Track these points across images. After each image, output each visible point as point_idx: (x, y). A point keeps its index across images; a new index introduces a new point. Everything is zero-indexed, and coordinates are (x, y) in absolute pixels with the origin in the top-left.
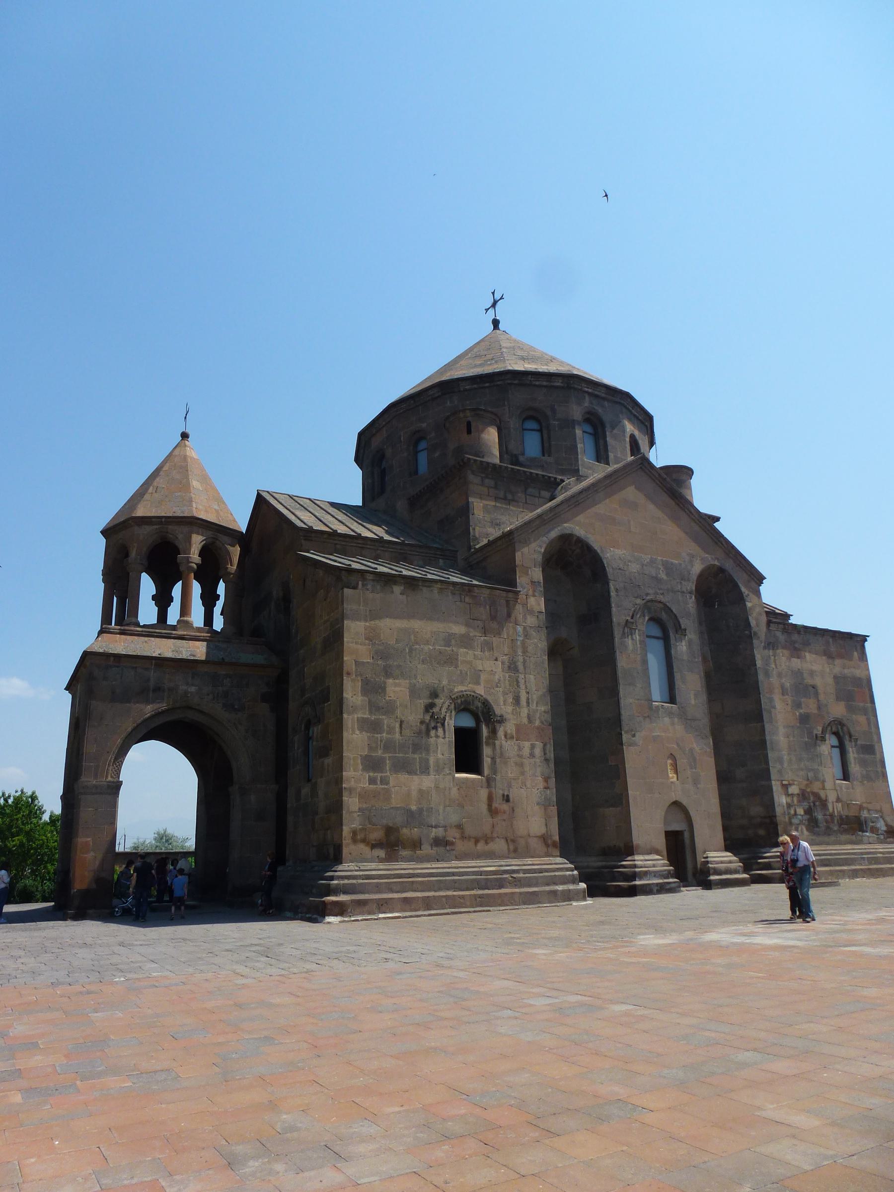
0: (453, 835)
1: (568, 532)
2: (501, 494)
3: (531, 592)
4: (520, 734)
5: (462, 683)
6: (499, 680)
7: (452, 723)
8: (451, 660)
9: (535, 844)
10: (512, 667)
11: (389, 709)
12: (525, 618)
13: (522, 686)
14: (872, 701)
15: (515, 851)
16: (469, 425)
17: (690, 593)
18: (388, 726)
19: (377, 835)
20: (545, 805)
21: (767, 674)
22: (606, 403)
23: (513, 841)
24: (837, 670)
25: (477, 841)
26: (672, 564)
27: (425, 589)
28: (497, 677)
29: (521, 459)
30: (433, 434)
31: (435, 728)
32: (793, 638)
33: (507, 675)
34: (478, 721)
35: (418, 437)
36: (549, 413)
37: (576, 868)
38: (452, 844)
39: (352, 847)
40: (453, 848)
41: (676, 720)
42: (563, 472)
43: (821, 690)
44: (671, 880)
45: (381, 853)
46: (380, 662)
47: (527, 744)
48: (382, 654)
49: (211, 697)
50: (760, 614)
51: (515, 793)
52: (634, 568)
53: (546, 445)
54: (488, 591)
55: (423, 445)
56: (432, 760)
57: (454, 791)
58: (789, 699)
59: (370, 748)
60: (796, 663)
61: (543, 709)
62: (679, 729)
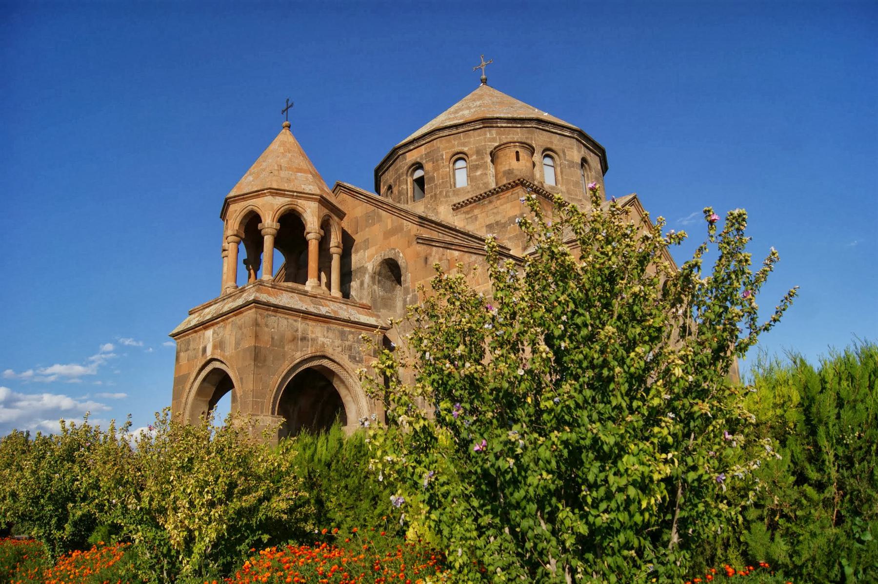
16: (517, 152)
22: (592, 154)
29: (545, 186)
30: (474, 157)
35: (460, 156)
36: (561, 155)
53: (560, 178)
55: (460, 164)
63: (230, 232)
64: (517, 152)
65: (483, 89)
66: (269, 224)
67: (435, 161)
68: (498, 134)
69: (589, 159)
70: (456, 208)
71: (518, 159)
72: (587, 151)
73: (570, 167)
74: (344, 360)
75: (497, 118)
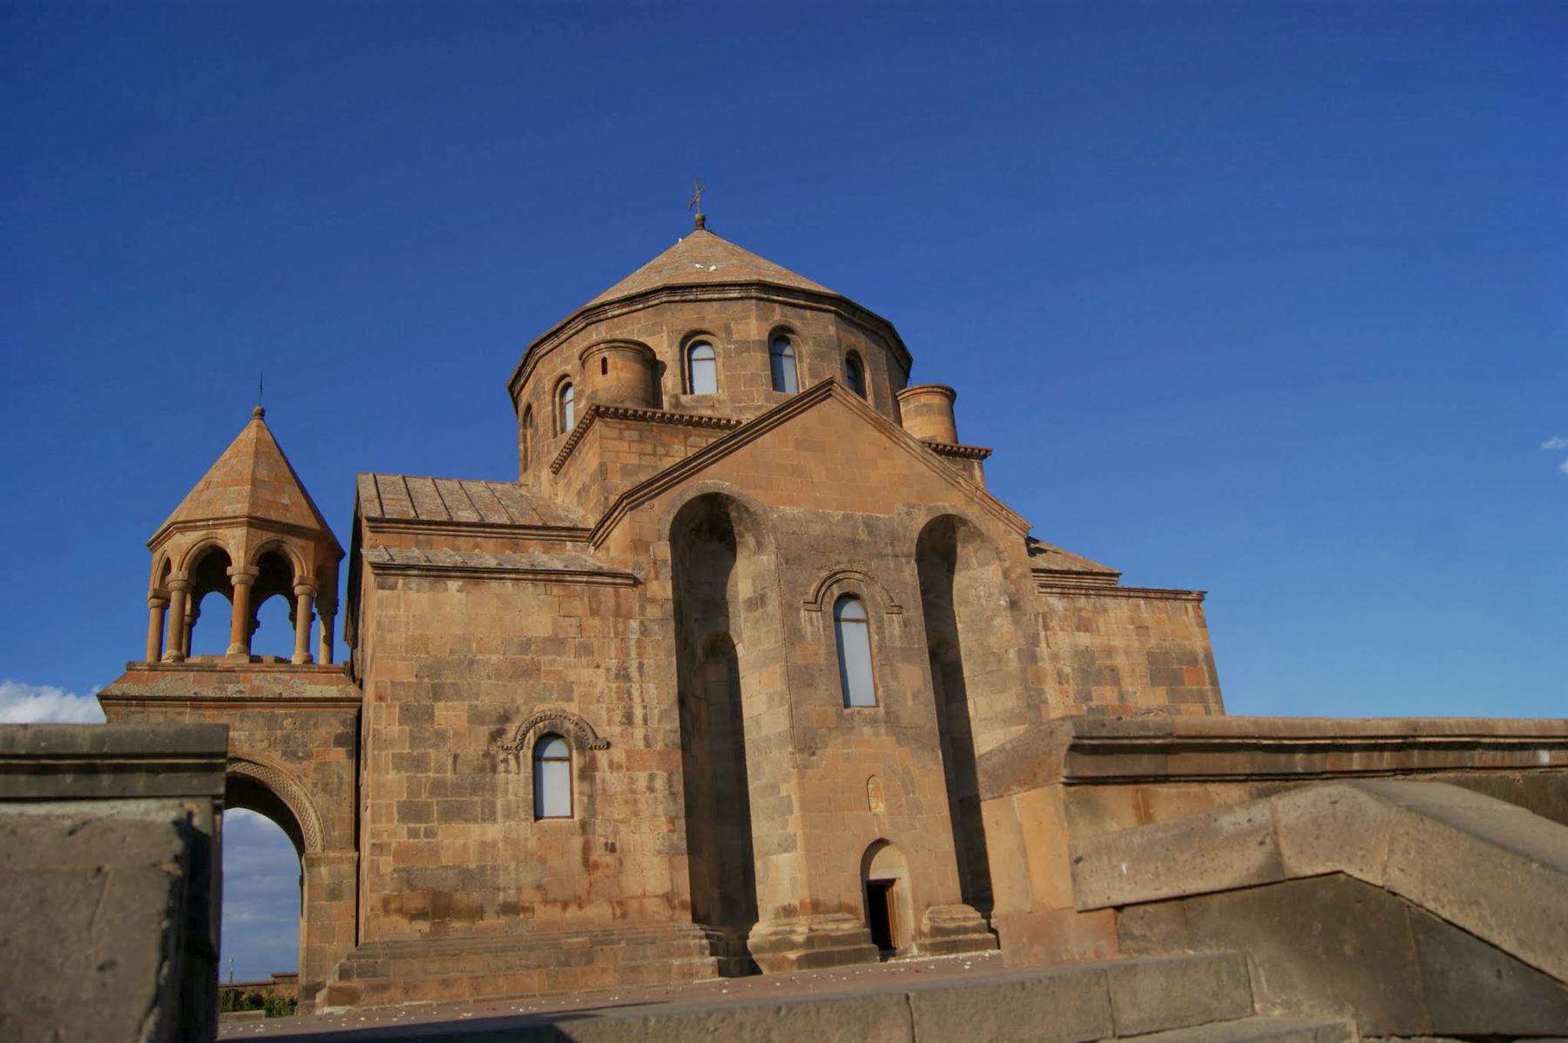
0: (530, 896)
2: (649, 449)
3: (652, 575)
4: (633, 761)
5: (543, 701)
7: (530, 753)
8: (533, 670)
9: (654, 907)
10: (623, 675)
11: (440, 736)
12: (643, 608)
13: (637, 699)
14: (1214, 681)
15: (624, 915)
16: (604, 360)
17: (908, 556)
18: (437, 761)
19: (416, 903)
20: (672, 853)
21: (1033, 657)
22: (808, 313)
23: (620, 903)
24: (1152, 642)
25: (565, 905)
26: (878, 519)
27: (493, 583)
28: (598, 690)
29: (684, 399)
31: (505, 761)
33: (614, 686)
34: (571, 751)
35: (563, 385)
37: (708, 936)
38: (525, 910)
39: (382, 919)
40: (529, 914)
41: (882, 729)
42: (741, 410)
43: (1124, 673)
44: (864, 946)
45: (424, 926)
46: (427, 680)
47: (642, 779)
49: (265, 743)
50: (1025, 576)
51: (627, 838)
52: (818, 528)
54: (585, 579)
55: (570, 394)
56: (500, 803)
57: (533, 843)
58: (1071, 688)
59: (411, 793)
60: (1084, 639)
61: (668, 727)
62: (886, 740)
63: (150, 594)
64: (604, 360)
65: (701, 236)
66: (177, 575)
67: (537, 398)
68: (610, 329)
69: (797, 324)
70: (557, 469)
71: (604, 372)
72: (789, 311)
73: (739, 352)
74: (276, 759)
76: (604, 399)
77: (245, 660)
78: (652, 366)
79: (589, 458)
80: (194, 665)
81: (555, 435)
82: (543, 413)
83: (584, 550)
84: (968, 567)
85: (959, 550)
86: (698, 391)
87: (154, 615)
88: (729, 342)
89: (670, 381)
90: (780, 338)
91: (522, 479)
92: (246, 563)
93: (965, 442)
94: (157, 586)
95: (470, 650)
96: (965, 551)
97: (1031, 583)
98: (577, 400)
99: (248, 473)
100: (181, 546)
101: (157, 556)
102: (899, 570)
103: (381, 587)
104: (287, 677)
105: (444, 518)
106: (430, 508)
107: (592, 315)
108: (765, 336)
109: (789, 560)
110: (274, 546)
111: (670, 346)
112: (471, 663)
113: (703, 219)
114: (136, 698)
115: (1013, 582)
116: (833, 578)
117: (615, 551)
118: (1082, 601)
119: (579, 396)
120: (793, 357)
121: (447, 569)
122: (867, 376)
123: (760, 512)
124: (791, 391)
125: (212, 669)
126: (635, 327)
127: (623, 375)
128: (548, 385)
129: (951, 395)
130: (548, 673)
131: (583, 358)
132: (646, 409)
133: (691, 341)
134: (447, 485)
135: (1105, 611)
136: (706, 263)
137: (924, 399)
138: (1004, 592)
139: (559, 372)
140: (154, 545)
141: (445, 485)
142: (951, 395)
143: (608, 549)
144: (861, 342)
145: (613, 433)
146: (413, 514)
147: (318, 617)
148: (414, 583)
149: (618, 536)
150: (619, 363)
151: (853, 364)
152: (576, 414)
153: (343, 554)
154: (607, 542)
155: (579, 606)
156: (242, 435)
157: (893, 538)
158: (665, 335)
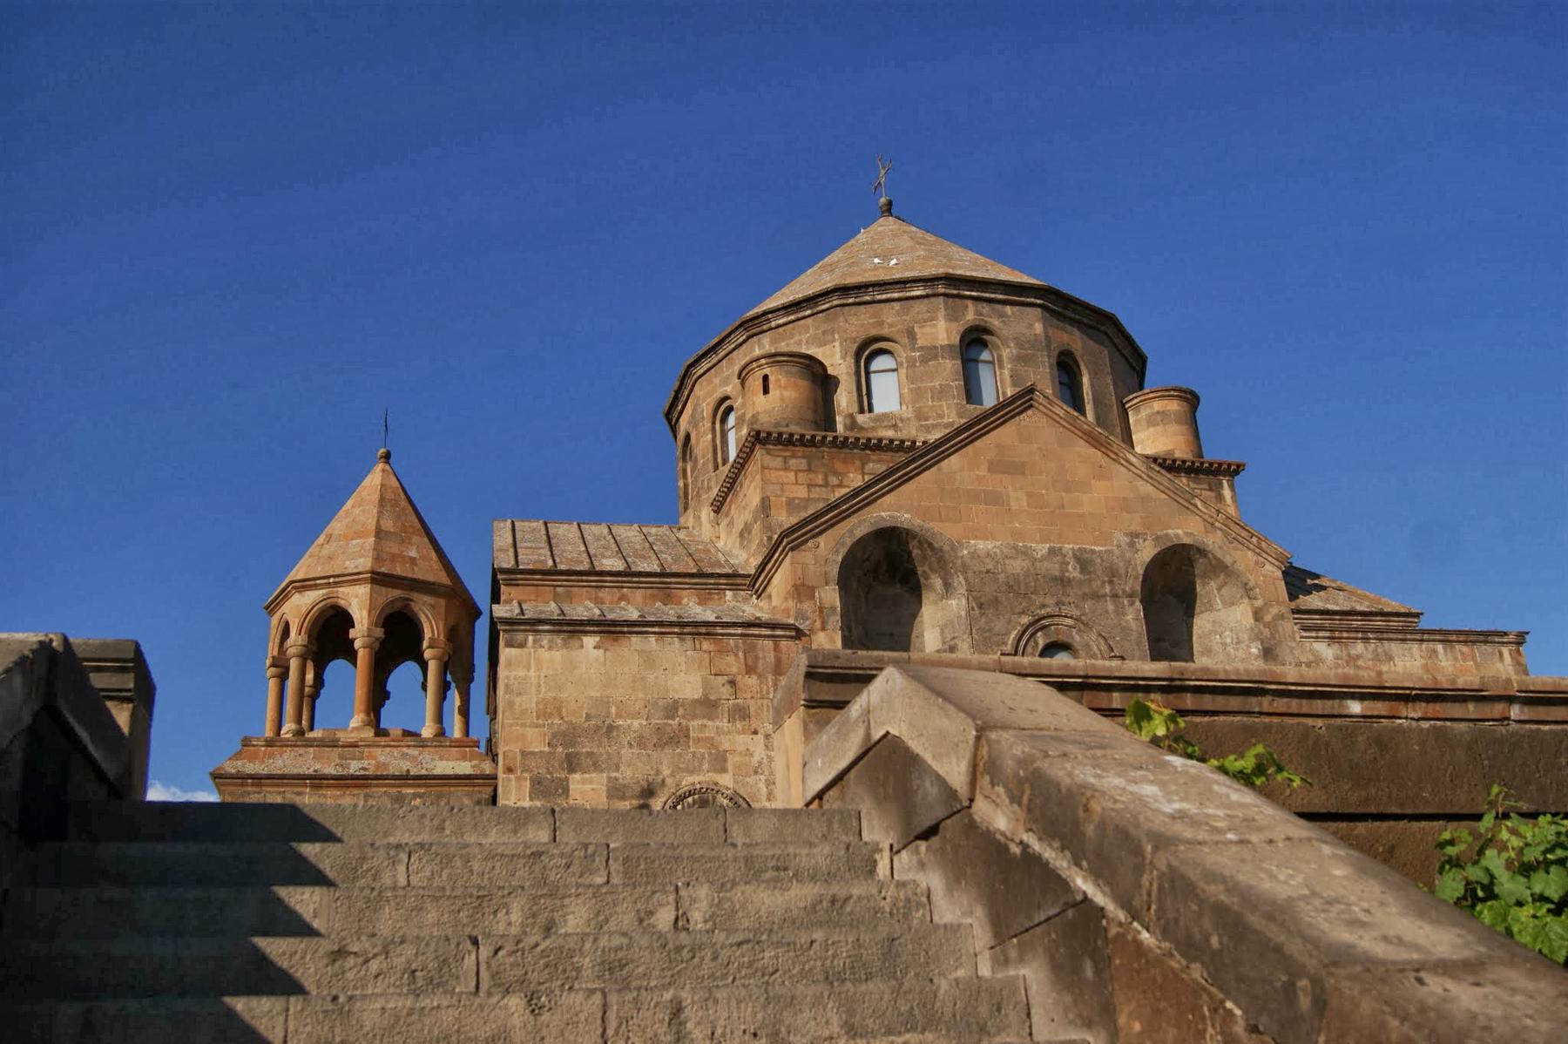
1: (889, 524)
2: (819, 479)
3: (818, 624)
5: (692, 773)
6: (760, 763)
8: (679, 738)
16: (766, 378)
17: (1131, 595)
22: (1008, 309)
26: (1093, 552)
27: (635, 639)
28: (756, 758)
29: (861, 419)
32: (1353, 652)
35: (723, 409)
42: (928, 429)
46: (560, 749)
48: (568, 737)
52: (1017, 566)
54: (739, 631)
63: (268, 662)
64: (766, 378)
65: (887, 225)
66: (296, 640)
67: (696, 426)
68: (774, 342)
69: (995, 323)
70: (718, 506)
71: (766, 391)
72: (986, 308)
73: (924, 361)
75: (765, 313)
76: (765, 423)
77: (369, 733)
78: (823, 382)
79: (751, 493)
80: (314, 739)
81: (716, 468)
82: (702, 444)
83: (746, 600)
84: (1210, 607)
85: (1198, 588)
86: (879, 408)
87: (273, 684)
88: (913, 349)
89: (844, 399)
90: (974, 341)
91: (682, 520)
92: (370, 624)
93: (1212, 455)
94: (275, 653)
95: (608, 715)
96: (1207, 589)
97: (1289, 626)
98: (738, 426)
99: (371, 523)
100: (300, 606)
101: (275, 620)
102: (1120, 612)
103: (509, 645)
104: (414, 752)
105: (585, 566)
106: (571, 554)
107: (753, 326)
108: (956, 340)
109: (982, 604)
110: (398, 605)
111: (844, 358)
112: (610, 729)
113: (890, 203)
114: (252, 777)
115: (1267, 625)
116: (1037, 625)
117: (776, 601)
118: (1359, 647)
119: (740, 420)
120: (992, 363)
121: (581, 623)
122: (1085, 380)
123: (946, 548)
124: (989, 401)
125: (333, 744)
126: (803, 338)
127: (787, 394)
128: (707, 408)
129: (1192, 400)
130: (699, 740)
131: (742, 376)
132: (817, 431)
133: (868, 351)
134: (594, 531)
135: (1391, 658)
136: (886, 257)
137: (1157, 405)
138: (1257, 637)
139: (718, 395)
140: (271, 608)
141: (591, 530)
142: (1192, 400)
143: (770, 596)
144: (1075, 340)
145: (778, 462)
146: (550, 563)
147: (453, 685)
148: (545, 640)
149: (780, 581)
150: (783, 381)
151: (1066, 367)
152: (737, 441)
153: (478, 613)
154: (769, 589)
155: (733, 664)
156: (367, 482)
157: (1112, 574)
158: (837, 344)
